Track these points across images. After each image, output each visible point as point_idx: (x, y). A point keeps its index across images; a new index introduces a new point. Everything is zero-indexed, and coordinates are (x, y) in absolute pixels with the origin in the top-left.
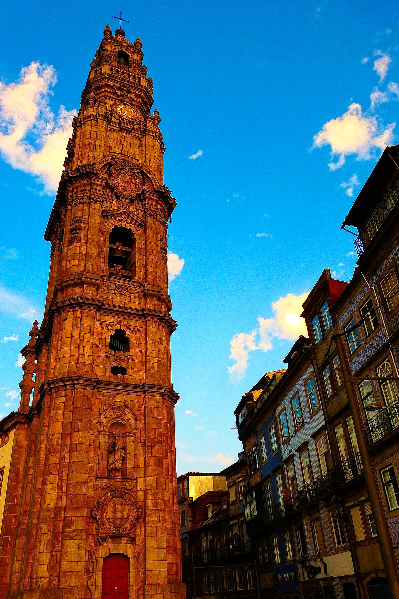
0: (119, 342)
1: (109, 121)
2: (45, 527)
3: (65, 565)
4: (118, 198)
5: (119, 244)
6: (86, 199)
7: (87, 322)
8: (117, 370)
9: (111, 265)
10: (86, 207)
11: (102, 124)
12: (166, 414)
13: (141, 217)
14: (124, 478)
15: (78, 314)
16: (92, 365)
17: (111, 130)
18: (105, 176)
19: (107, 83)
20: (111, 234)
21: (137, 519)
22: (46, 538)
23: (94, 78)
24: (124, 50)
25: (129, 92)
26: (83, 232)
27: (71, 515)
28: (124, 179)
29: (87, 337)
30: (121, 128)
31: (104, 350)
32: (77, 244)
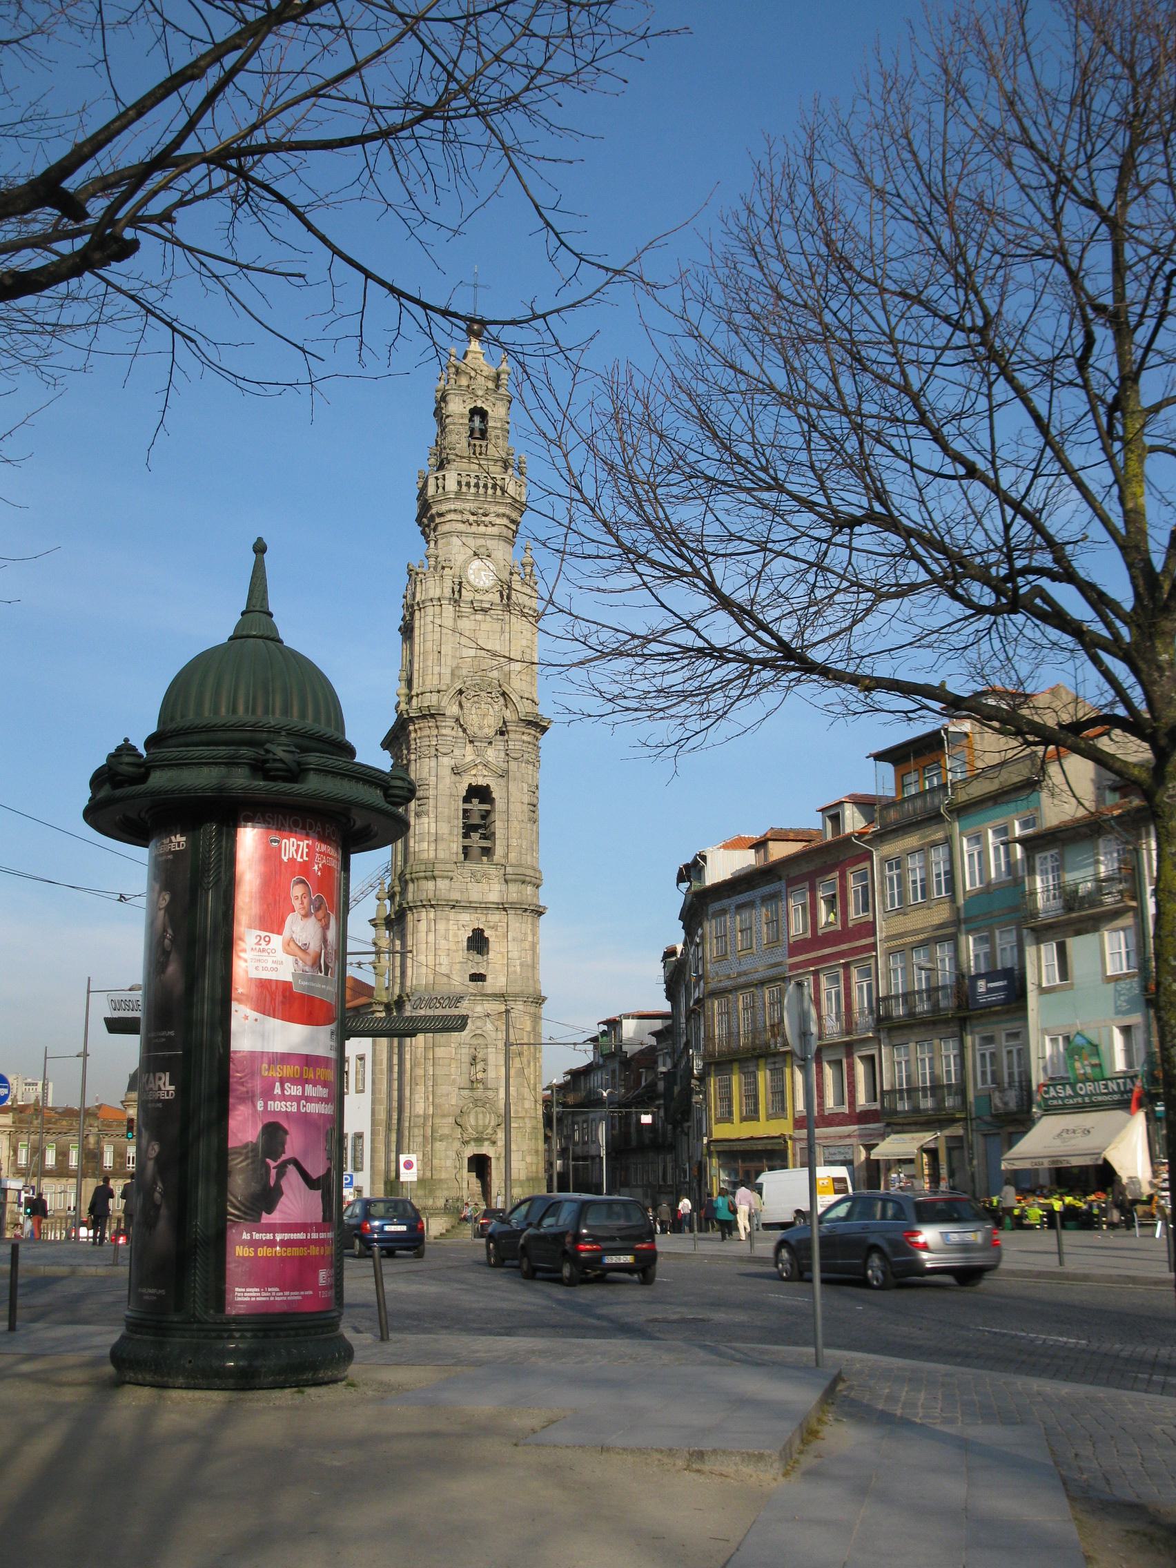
0: (478, 942)
1: (456, 602)
2: (416, 1131)
4: (471, 742)
5: (476, 801)
6: (433, 752)
7: (441, 926)
8: (477, 977)
9: (466, 835)
10: (433, 763)
11: (449, 610)
12: (529, 1023)
13: (502, 764)
14: (486, 1089)
17: (459, 616)
19: (453, 507)
20: (466, 800)
22: (420, 1139)
25: (486, 515)
26: (432, 802)
28: (479, 712)
29: (443, 944)
32: (425, 820)
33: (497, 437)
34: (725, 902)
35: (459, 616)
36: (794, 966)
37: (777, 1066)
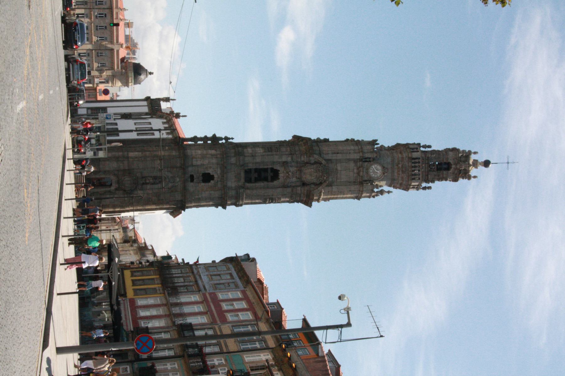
0: (207, 178)
2: (121, 154)
3: (107, 162)
5: (272, 174)
7: (214, 161)
8: (192, 178)
9: (256, 170)
11: (357, 156)
15: (218, 156)
16: (192, 166)
18: (313, 162)
19: (405, 156)
21: (125, 191)
23: (408, 148)
24: (453, 166)
25: (402, 171)
26: (270, 153)
27: (126, 162)
29: (206, 162)
30: (360, 167)
31: (202, 170)
33: (439, 176)
34: (233, 269)
35: (355, 161)
36: (204, 295)
37: (158, 291)
